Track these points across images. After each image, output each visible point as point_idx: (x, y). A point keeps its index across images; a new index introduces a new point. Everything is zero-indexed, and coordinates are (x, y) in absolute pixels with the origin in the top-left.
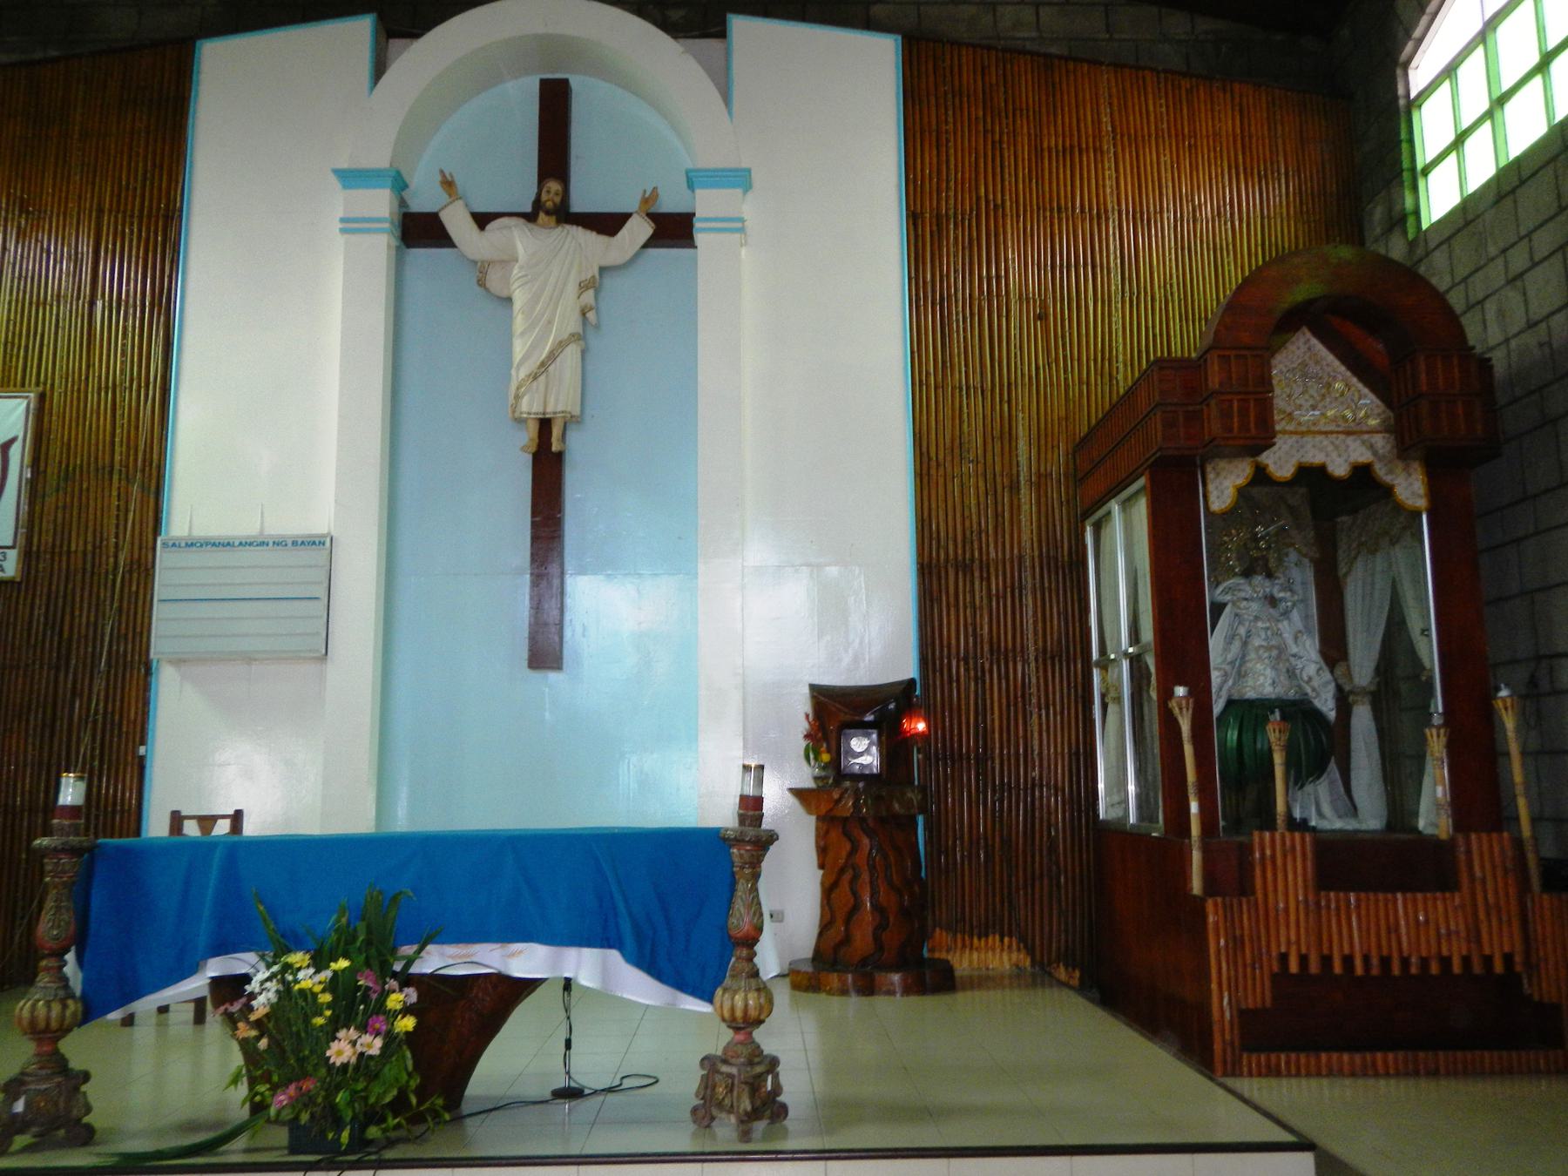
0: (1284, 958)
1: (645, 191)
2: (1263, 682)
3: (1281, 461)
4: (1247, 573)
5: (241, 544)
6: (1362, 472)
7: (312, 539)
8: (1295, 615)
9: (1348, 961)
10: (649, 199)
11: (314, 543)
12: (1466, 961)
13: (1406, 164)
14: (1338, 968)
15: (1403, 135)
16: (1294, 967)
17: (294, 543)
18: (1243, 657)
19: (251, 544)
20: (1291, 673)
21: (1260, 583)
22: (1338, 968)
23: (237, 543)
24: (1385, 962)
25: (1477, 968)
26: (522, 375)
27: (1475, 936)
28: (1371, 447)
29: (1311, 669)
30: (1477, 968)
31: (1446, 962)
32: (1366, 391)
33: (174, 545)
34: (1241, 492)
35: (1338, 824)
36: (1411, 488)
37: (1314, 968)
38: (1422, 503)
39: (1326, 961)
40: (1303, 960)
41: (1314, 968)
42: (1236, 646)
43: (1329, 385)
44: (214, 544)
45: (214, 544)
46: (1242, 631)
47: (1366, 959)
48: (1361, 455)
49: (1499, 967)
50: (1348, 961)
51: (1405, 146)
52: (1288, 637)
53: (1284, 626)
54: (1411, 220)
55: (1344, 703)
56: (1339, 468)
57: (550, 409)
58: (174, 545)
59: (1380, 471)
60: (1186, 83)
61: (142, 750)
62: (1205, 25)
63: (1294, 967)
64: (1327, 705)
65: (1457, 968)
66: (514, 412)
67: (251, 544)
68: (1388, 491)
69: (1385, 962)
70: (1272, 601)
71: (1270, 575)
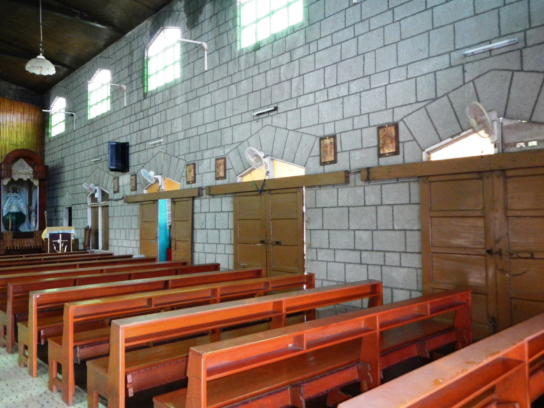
0: (7, 248)
2: (14, 209)
3: (16, 178)
4: (13, 192)
6: (29, 180)
8: (21, 199)
9: (17, 248)
12: (34, 247)
13: (50, 125)
14: (15, 248)
15: (50, 120)
16: (9, 248)
18: (11, 204)
20: (19, 208)
21: (15, 194)
22: (15, 248)
24: (22, 247)
25: (36, 247)
27: (36, 242)
28: (30, 176)
29: (23, 207)
30: (36, 247)
31: (31, 247)
32: (30, 167)
34: (9, 182)
35: (28, 231)
36: (36, 183)
37: (12, 248)
38: (37, 185)
39: (14, 248)
40: (10, 248)
41: (12, 248)
42: (10, 204)
43: (24, 167)
46: (11, 201)
47: (20, 247)
48: (29, 177)
49: (39, 247)
50: (17, 248)
51: (50, 122)
52: (19, 202)
53: (19, 201)
54: (50, 134)
55: (30, 213)
56: (25, 179)
59: (32, 180)
60: (13, 101)
62: (19, 88)
63: (9, 248)
64: (25, 212)
65: (33, 248)
68: (32, 183)
69: (22, 247)
70: (16, 197)
71: (17, 192)
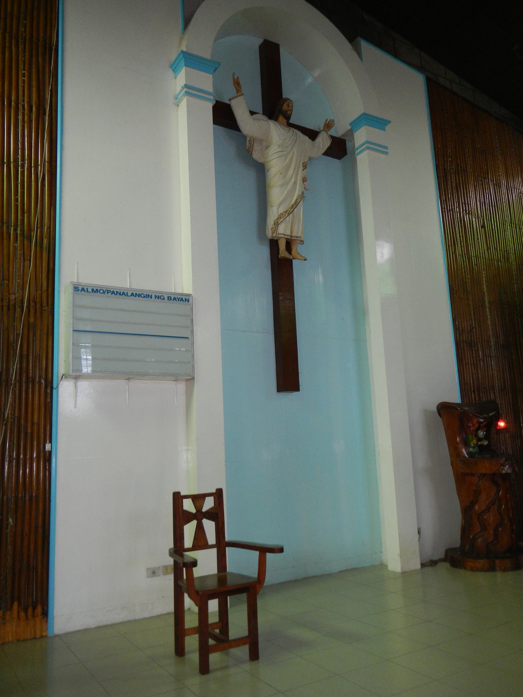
1: (327, 120)
5: (132, 294)
7: (181, 297)
10: (328, 125)
11: (182, 299)
17: (169, 298)
19: (139, 296)
23: (129, 294)
26: (282, 210)
33: (83, 289)
44: (113, 293)
45: (113, 293)
57: (293, 235)
58: (83, 289)
61: (48, 447)
66: (273, 233)
67: (139, 296)
